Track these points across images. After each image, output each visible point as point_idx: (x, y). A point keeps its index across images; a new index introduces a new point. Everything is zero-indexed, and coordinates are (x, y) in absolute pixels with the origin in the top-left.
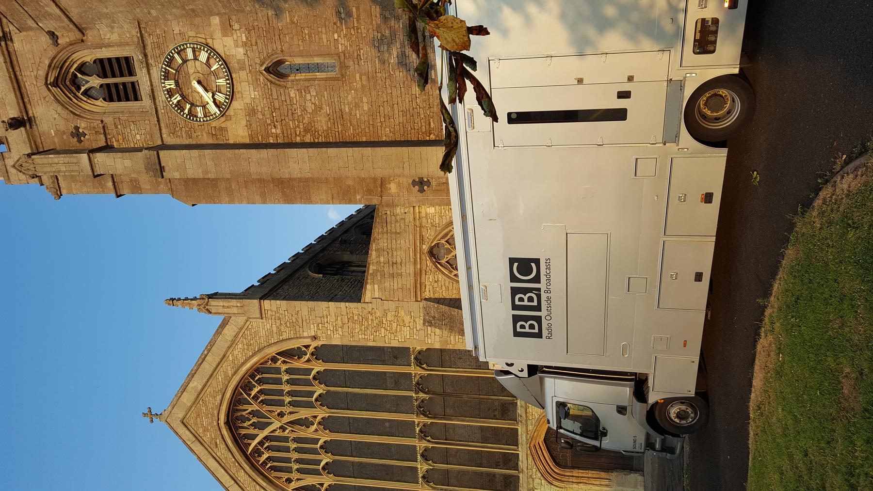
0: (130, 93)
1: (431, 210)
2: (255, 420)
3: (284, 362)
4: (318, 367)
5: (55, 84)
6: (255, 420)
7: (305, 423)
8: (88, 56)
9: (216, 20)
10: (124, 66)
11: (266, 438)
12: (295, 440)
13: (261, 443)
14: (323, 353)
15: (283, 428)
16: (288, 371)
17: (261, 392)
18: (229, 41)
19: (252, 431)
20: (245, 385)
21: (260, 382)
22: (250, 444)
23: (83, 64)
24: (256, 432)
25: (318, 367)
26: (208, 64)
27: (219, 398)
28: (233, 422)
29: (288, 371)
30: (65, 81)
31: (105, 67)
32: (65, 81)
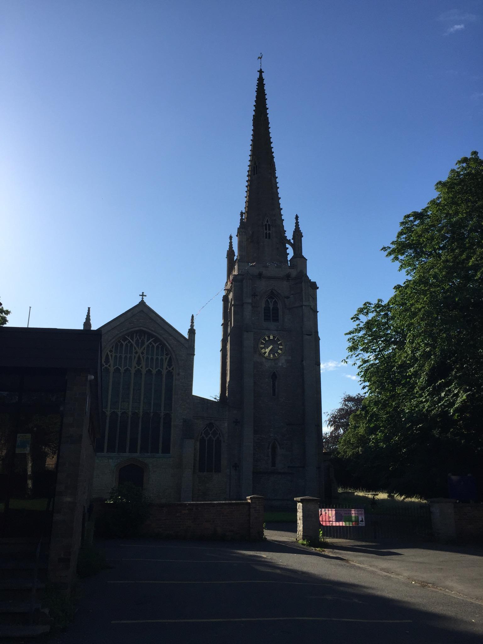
0: (267, 318)
1: (226, 425)
2: (140, 341)
3: (166, 358)
4: (164, 372)
5: (272, 291)
6: (140, 341)
7: (139, 363)
8: (280, 306)
9: (290, 358)
10: (276, 319)
11: (132, 345)
12: (130, 357)
13: (129, 342)
14: (170, 375)
15: (136, 353)
16: (162, 359)
17: (153, 346)
18: (283, 361)
19: (135, 340)
20: (157, 340)
21: (158, 347)
22: (128, 336)
23: (277, 303)
24: (135, 340)
25: (164, 372)
26: (277, 352)
27: (153, 329)
28: (141, 333)
29: (162, 359)
30: (272, 295)
31: (276, 310)
32: (272, 295)
